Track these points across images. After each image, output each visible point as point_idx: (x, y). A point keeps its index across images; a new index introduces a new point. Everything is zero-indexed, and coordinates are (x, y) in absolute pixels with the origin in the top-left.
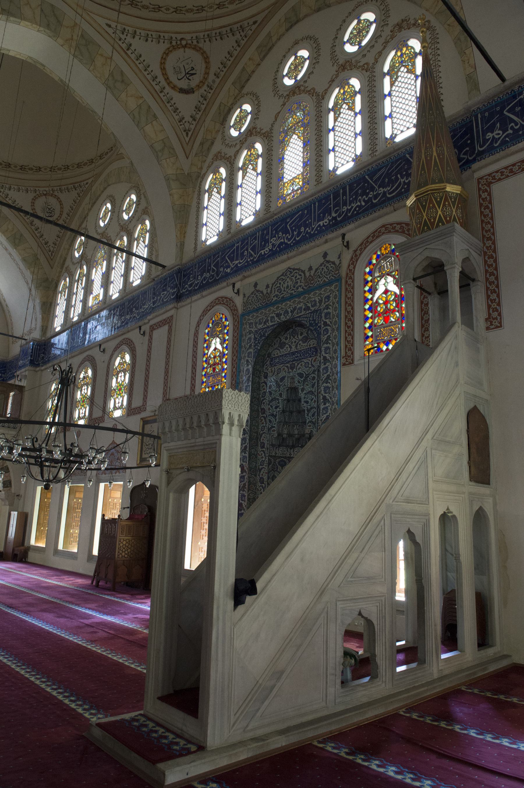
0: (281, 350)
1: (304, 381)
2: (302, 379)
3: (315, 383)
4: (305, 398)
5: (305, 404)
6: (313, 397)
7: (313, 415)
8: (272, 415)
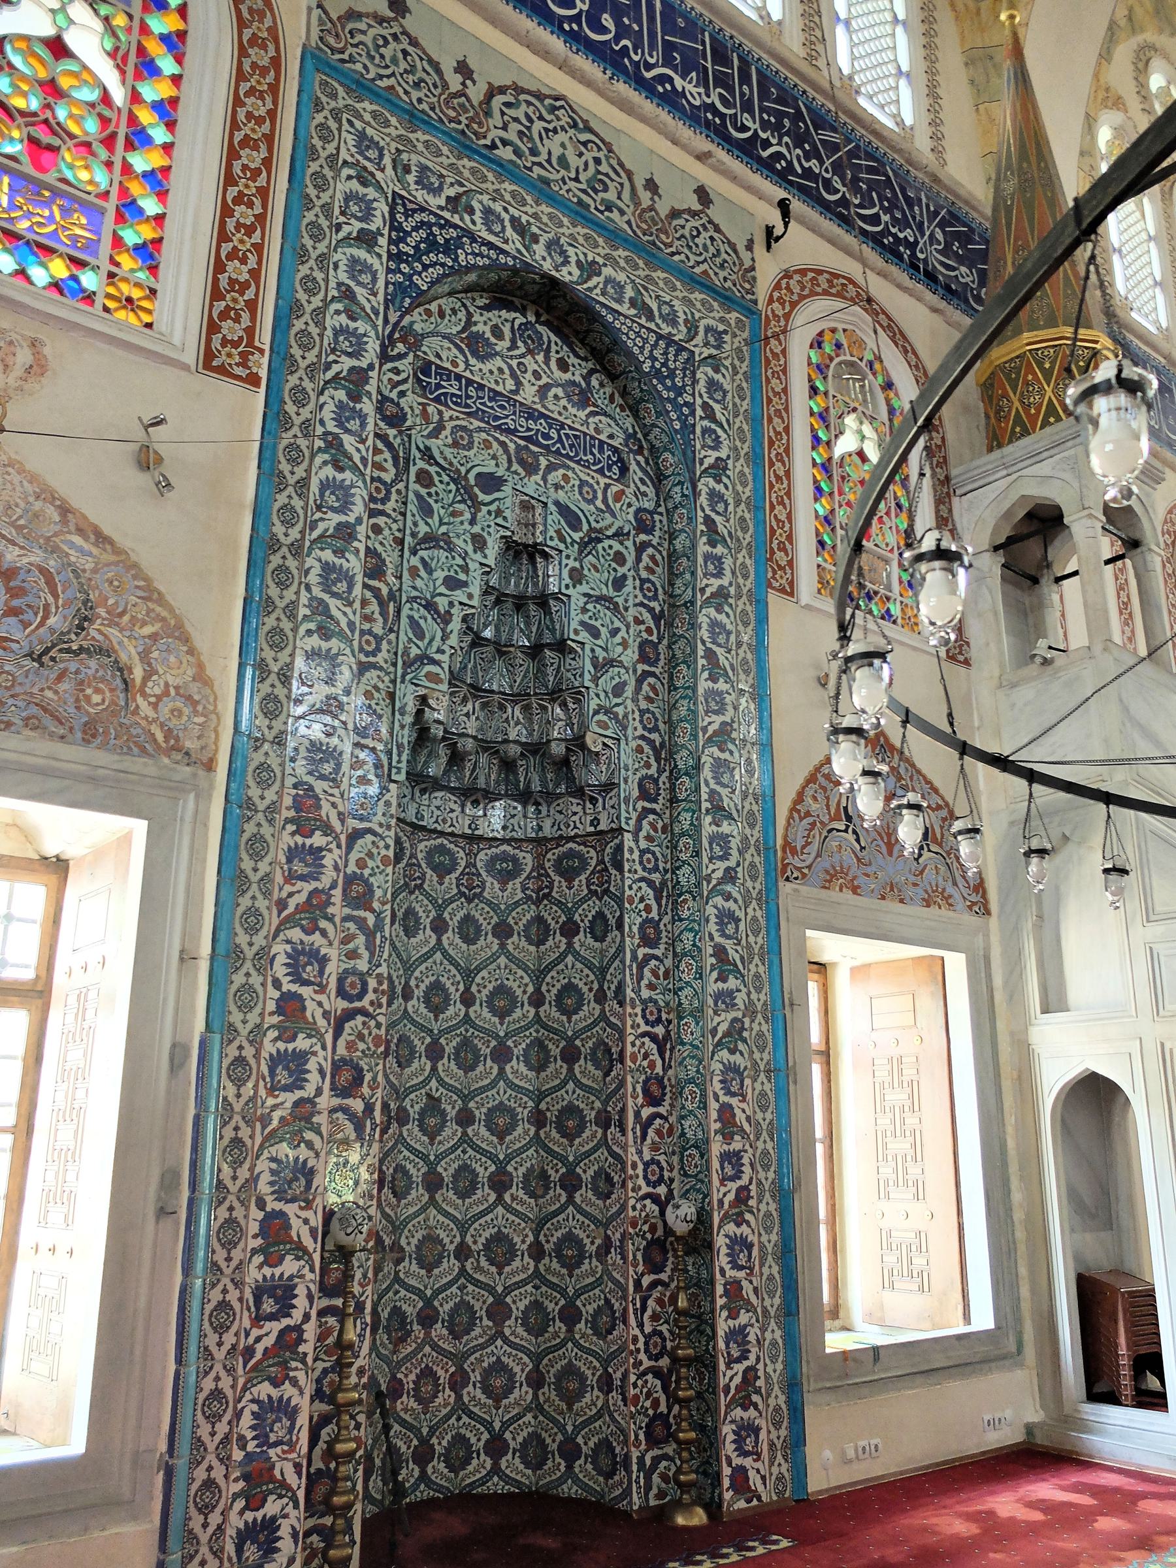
0: (472, 361)
1: (583, 545)
2: (577, 536)
3: (624, 577)
4: (584, 610)
5: (584, 636)
6: (617, 624)
7: (618, 690)
8: (430, 606)
